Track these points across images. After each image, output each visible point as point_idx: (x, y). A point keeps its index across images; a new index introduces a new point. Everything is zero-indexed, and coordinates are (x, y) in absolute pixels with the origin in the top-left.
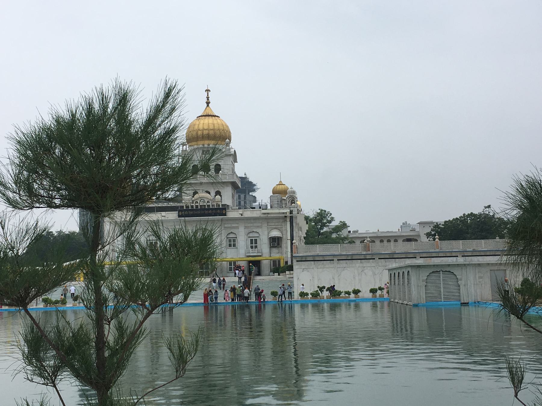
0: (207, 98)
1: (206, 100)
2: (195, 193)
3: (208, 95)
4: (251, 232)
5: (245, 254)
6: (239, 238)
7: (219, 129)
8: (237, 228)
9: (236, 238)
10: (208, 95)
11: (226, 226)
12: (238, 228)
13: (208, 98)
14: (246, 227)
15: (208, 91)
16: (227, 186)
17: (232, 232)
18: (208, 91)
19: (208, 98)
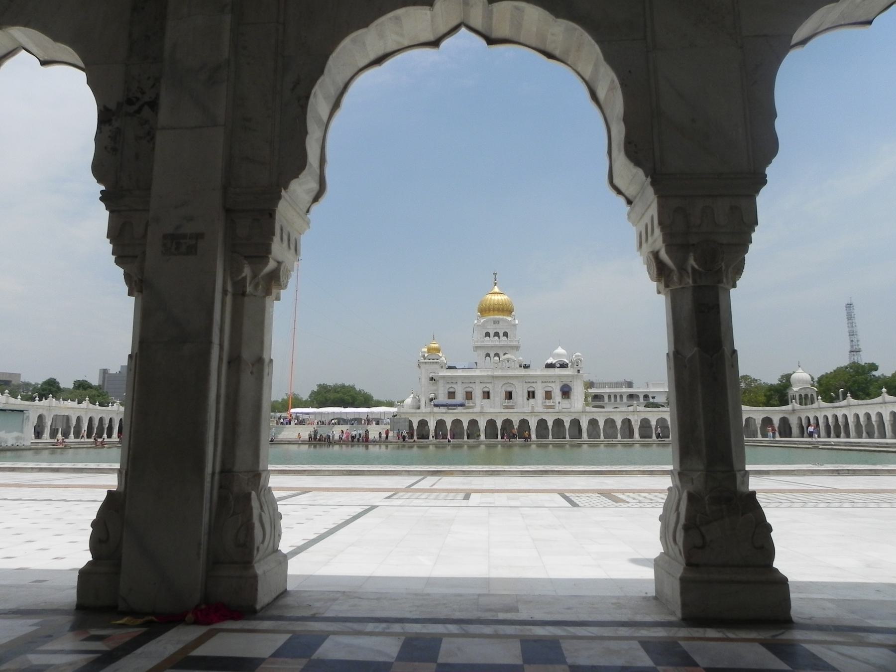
2: (504, 354)
4: (546, 387)
5: (542, 403)
7: (506, 304)
16: (513, 349)
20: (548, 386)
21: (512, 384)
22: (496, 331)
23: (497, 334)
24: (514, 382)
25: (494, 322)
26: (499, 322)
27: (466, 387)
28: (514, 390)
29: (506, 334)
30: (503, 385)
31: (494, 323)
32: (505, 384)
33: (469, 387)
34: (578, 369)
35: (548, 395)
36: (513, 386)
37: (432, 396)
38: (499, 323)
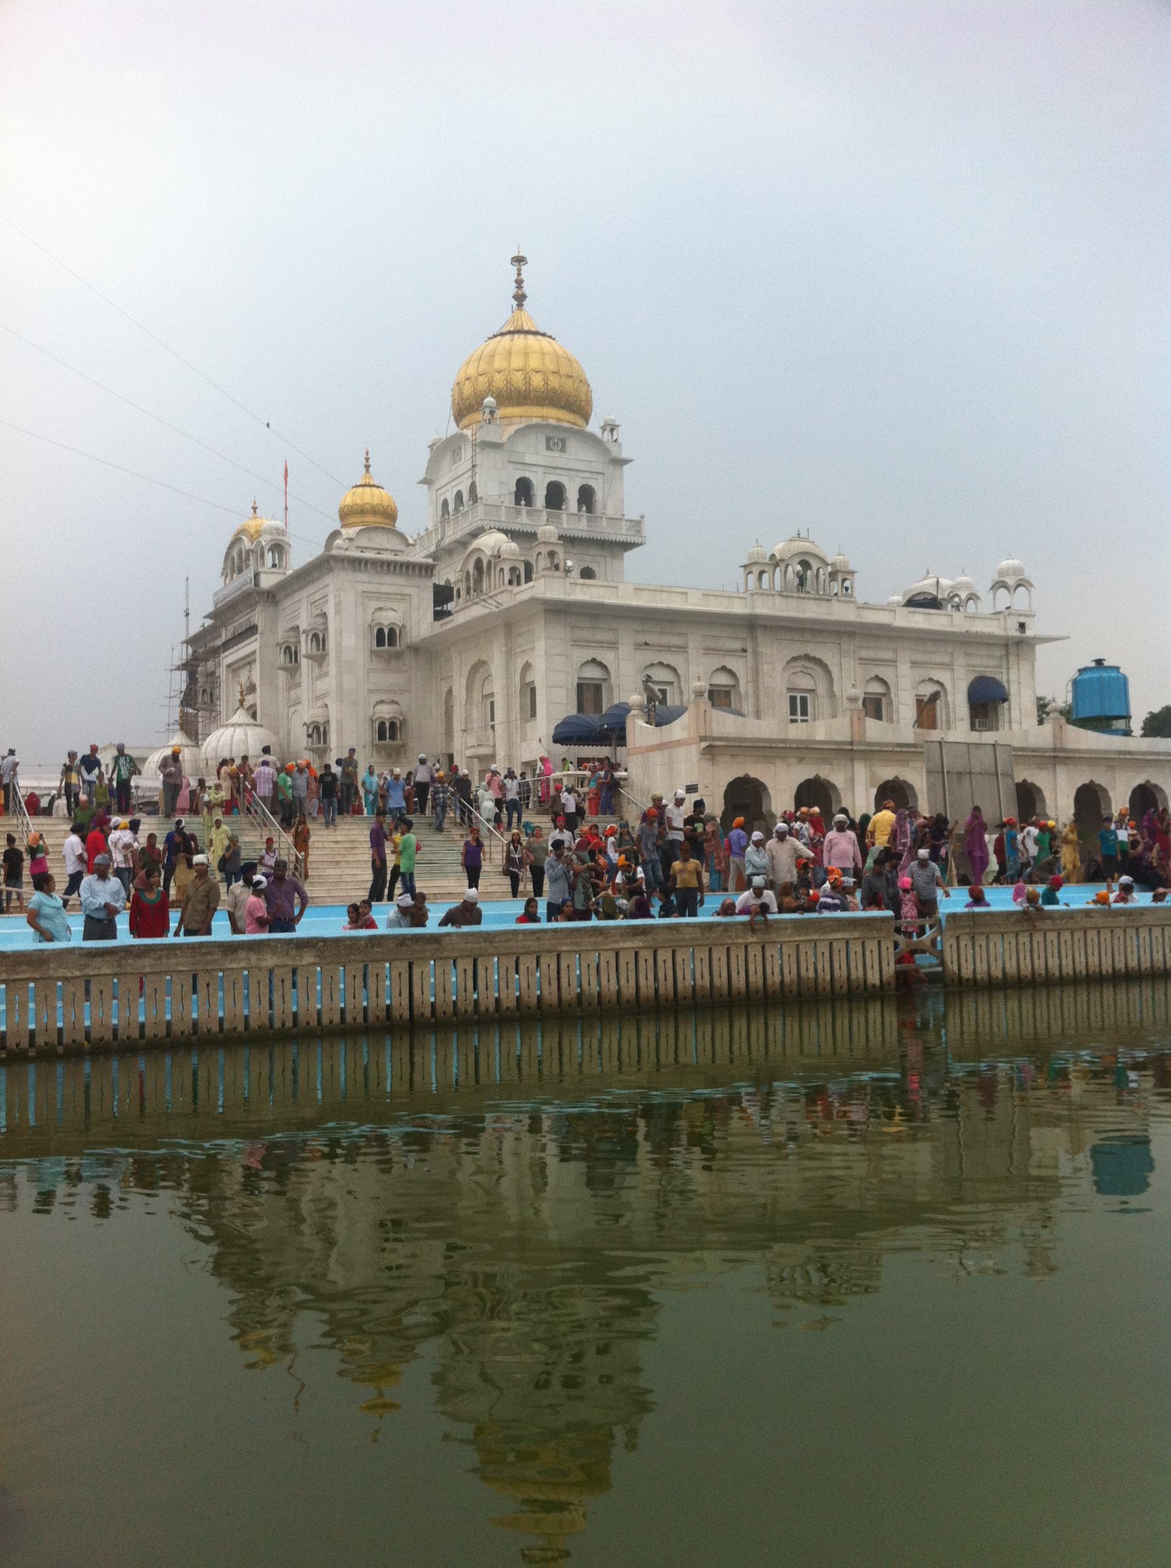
0: (516, 281)
1: (513, 289)
3: (519, 274)
4: (924, 681)
6: (897, 695)
8: (893, 662)
9: (887, 694)
10: (519, 274)
11: (864, 654)
12: (893, 662)
13: (519, 283)
14: (915, 664)
15: (519, 260)
17: (877, 678)
18: (519, 260)
19: (519, 283)
20: (931, 680)
21: (819, 662)
22: (553, 478)
23: (555, 496)
24: (826, 653)
25: (548, 439)
26: (563, 441)
27: (652, 665)
28: (822, 690)
29: (586, 496)
30: (788, 662)
31: (548, 448)
32: (794, 659)
33: (661, 664)
34: (1022, 620)
35: (927, 712)
36: (818, 671)
37: (386, 712)
38: (563, 450)
